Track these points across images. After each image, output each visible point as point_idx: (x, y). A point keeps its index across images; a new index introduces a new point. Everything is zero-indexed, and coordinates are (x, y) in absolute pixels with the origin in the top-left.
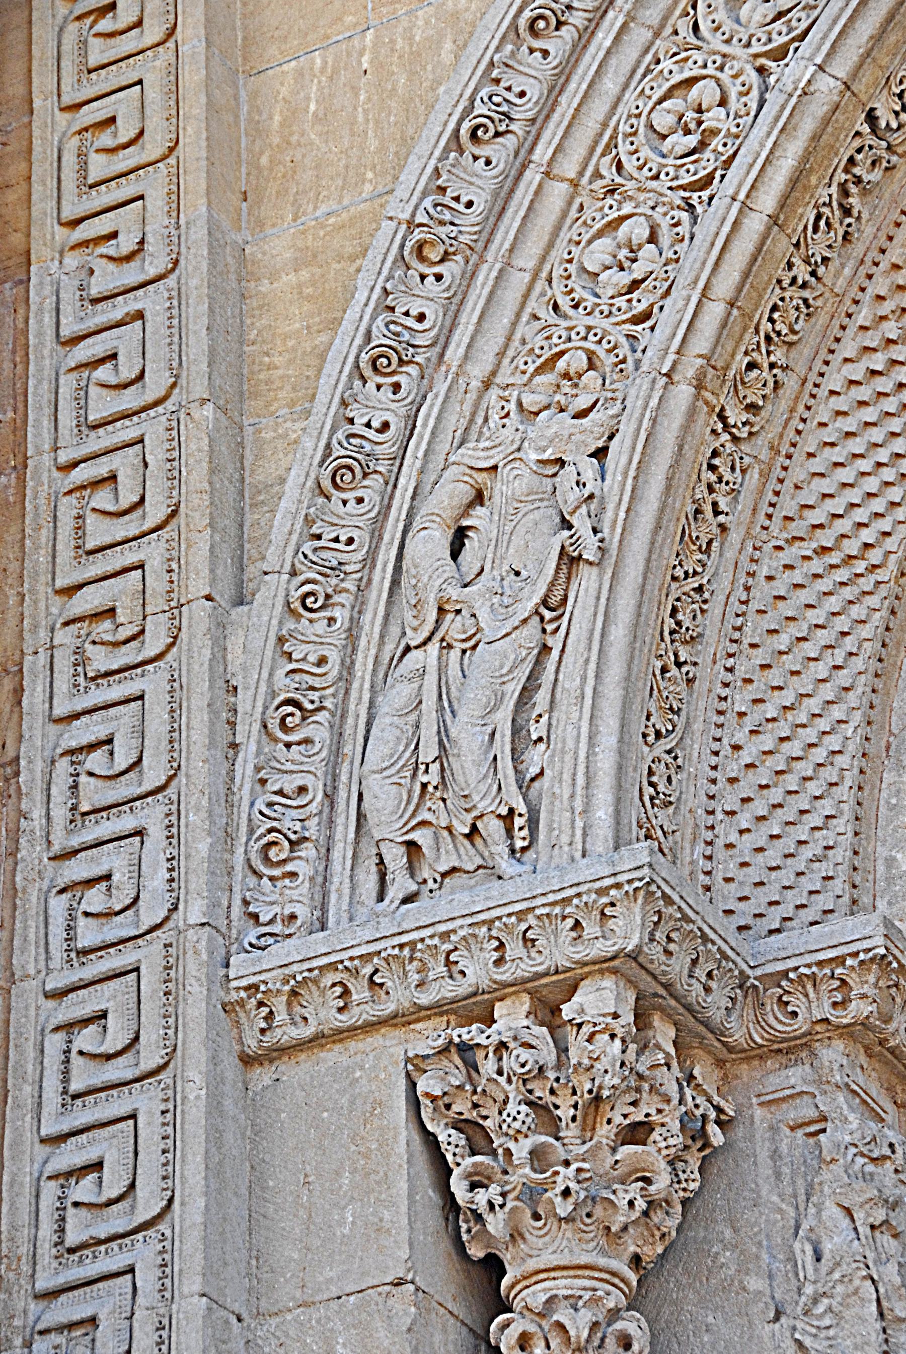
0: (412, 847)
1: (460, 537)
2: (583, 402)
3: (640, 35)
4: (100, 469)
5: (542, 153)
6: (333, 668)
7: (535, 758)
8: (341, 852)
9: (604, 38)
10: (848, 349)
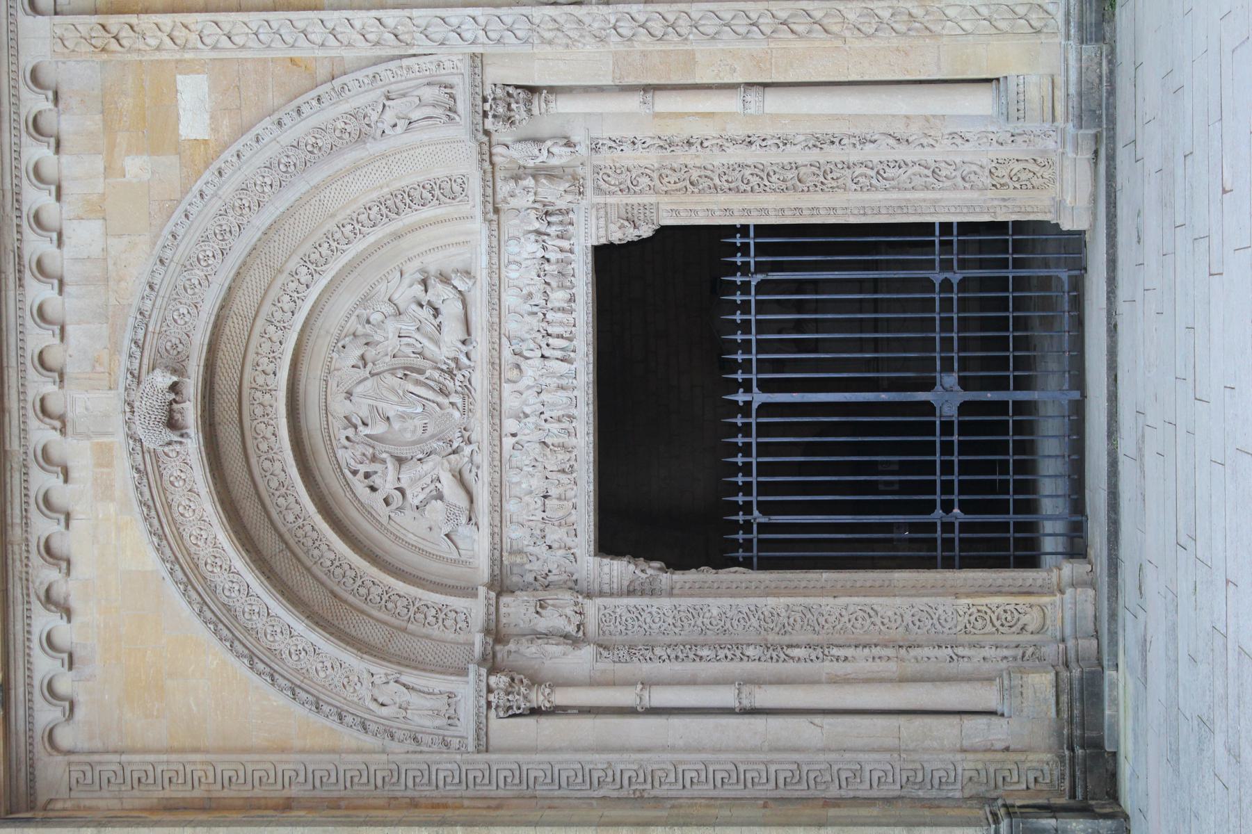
0: (449, 718)
1: (383, 705)
2: (356, 679)
3: (276, 660)
4: (348, 780)
5: (298, 683)
6: (406, 732)
7: (436, 691)
8: (446, 733)
9: (276, 667)
10: (348, 630)
